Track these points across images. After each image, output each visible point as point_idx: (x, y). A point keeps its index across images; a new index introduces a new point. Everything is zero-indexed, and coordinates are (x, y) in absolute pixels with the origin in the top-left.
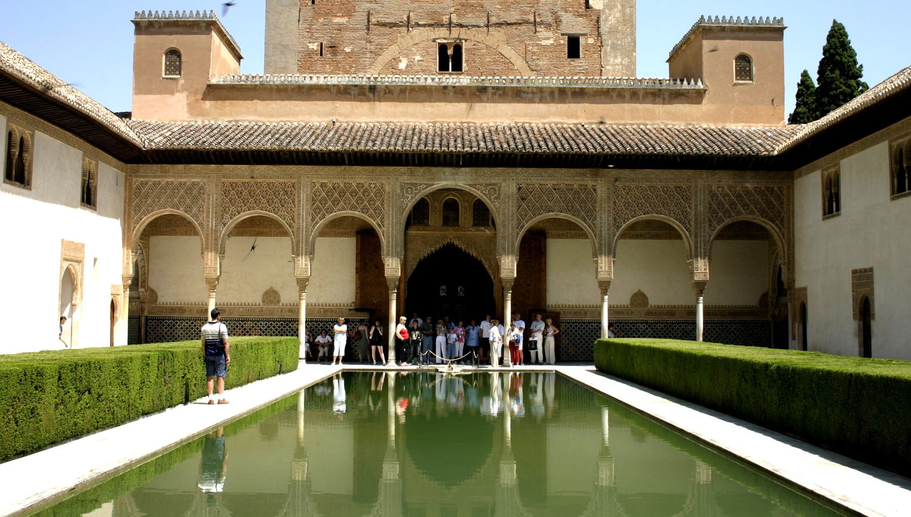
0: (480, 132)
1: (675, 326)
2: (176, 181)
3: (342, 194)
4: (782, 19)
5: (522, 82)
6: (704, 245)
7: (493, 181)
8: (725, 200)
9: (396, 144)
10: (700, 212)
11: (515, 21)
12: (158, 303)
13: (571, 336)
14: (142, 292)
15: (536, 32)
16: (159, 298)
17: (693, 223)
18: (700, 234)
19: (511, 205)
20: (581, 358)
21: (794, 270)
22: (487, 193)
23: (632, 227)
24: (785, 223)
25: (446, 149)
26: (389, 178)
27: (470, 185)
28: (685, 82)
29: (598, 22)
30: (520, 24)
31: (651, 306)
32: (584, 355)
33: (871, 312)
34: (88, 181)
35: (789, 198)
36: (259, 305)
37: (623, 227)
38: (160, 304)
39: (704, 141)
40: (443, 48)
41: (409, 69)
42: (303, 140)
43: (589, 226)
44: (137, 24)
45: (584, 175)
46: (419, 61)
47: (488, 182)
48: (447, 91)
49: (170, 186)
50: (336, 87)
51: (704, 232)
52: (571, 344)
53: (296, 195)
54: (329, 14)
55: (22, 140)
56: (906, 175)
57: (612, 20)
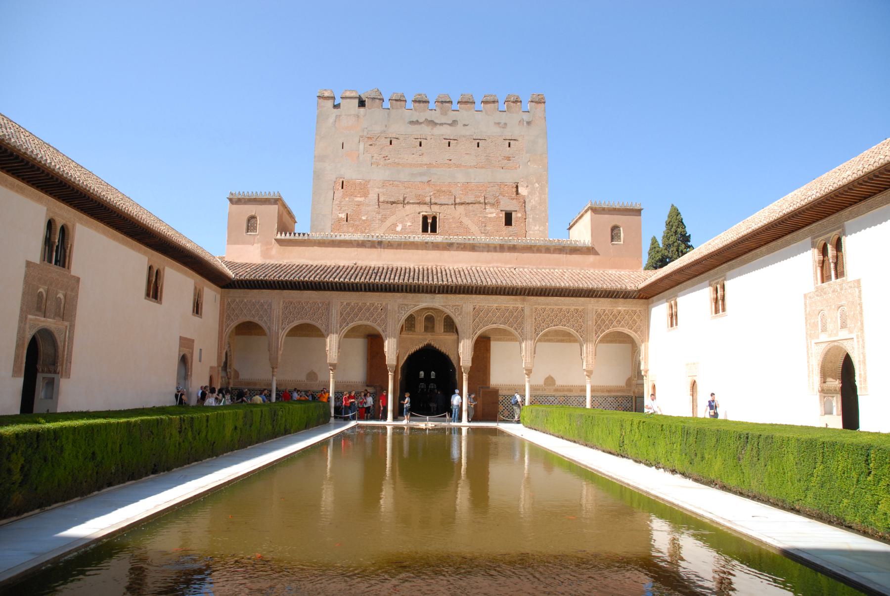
0: (448, 271)
1: (573, 399)
7: (457, 304)
9: (394, 279)
10: (590, 325)
11: (472, 202)
14: (230, 372)
15: (485, 209)
18: (590, 339)
19: (468, 319)
21: (648, 363)
23: (546, 335)
25: (427, 282)
26: (390, 301)
27: (442, 306)
29: (525, 203)
30: (475, 203)
31: (557, 386)
40: (425, 218)
42: (335, 274)
43: (519, 333)
44: (231, 200)
45: (516, 300)
46: (409, 226)
48: (427, 245)
52: (506, 410)
54: (352, 195)
55: (157, 271)
57: (533, 202)
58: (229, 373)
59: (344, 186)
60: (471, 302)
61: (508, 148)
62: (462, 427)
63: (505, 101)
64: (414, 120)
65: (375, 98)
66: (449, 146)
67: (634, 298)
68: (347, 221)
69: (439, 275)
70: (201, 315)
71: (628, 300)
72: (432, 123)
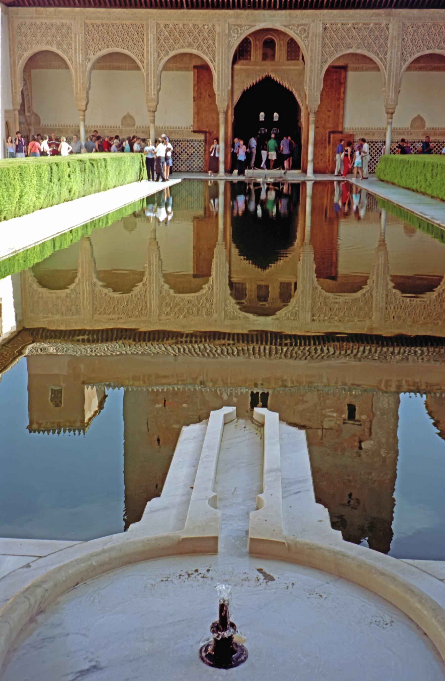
2: (48, 21)
3: (182, 34)
7: (304, 22)
12: (41, 125)
14: (29, 116)
19: (317, 43)
22: (298, 32)
26: (219, 20)
27: (285, 26)
36: (119, 127)
37: (409, 61)
38: (42, 126)
43: (381, 59)
45: (379, 15)
47: (300, 23)
49: (44, 26)
53: (145, 35)
58: (27, 118)
62: (306, 181)
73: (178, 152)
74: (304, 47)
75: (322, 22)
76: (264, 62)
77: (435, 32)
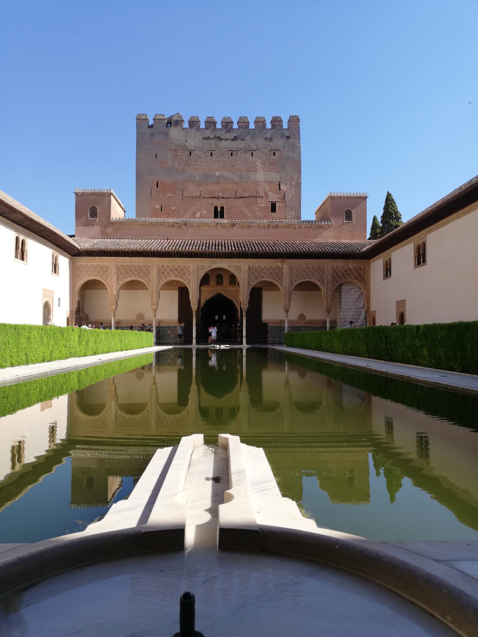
1: (317, 329)
4: (366, 193)
5: (251, 222)
6: (331, 292)
7: (238, 265)
8: (340, 273)
11: (247, 196)
12: (89, 320)
13: (272, 333)
14: (82, 315)
16: (89, 318)
17: (325, 283)
18: (329, 287)
20: (277, 342)
24: (366, 283)
27: (228, 266)
28: (323, 222)
29: (285, 196)
32: (278, 341)
33: (405, 319)
34: (55, 263)
35: (368, 271)
36: (135, 320)
38: (90, 320)
39: (331, 247)
40: (216, 208)
41: (201, 217)
43: (280, 284)
46: (205, 213)
47: (236, 265)
48: (217, 226)
50: (168, 223)
51: (330, 287)
56: (422, 257)
57: (290, 195)
59: (159, 186)
60: (247, 263)
61: (273, 157)
63: (271, 122)
64: (207, 137)
65: (178, 120)
66: (232, 155)
67: (360, 259)
68: (161, 210)
69: (226, 245)
70: (58, 274)
71: (356, 260)
72: (220, 139)
73: (169, 333)
74: (239, 277)
75: (248, 265)
76: (217, 286)
77: (307, 270)
